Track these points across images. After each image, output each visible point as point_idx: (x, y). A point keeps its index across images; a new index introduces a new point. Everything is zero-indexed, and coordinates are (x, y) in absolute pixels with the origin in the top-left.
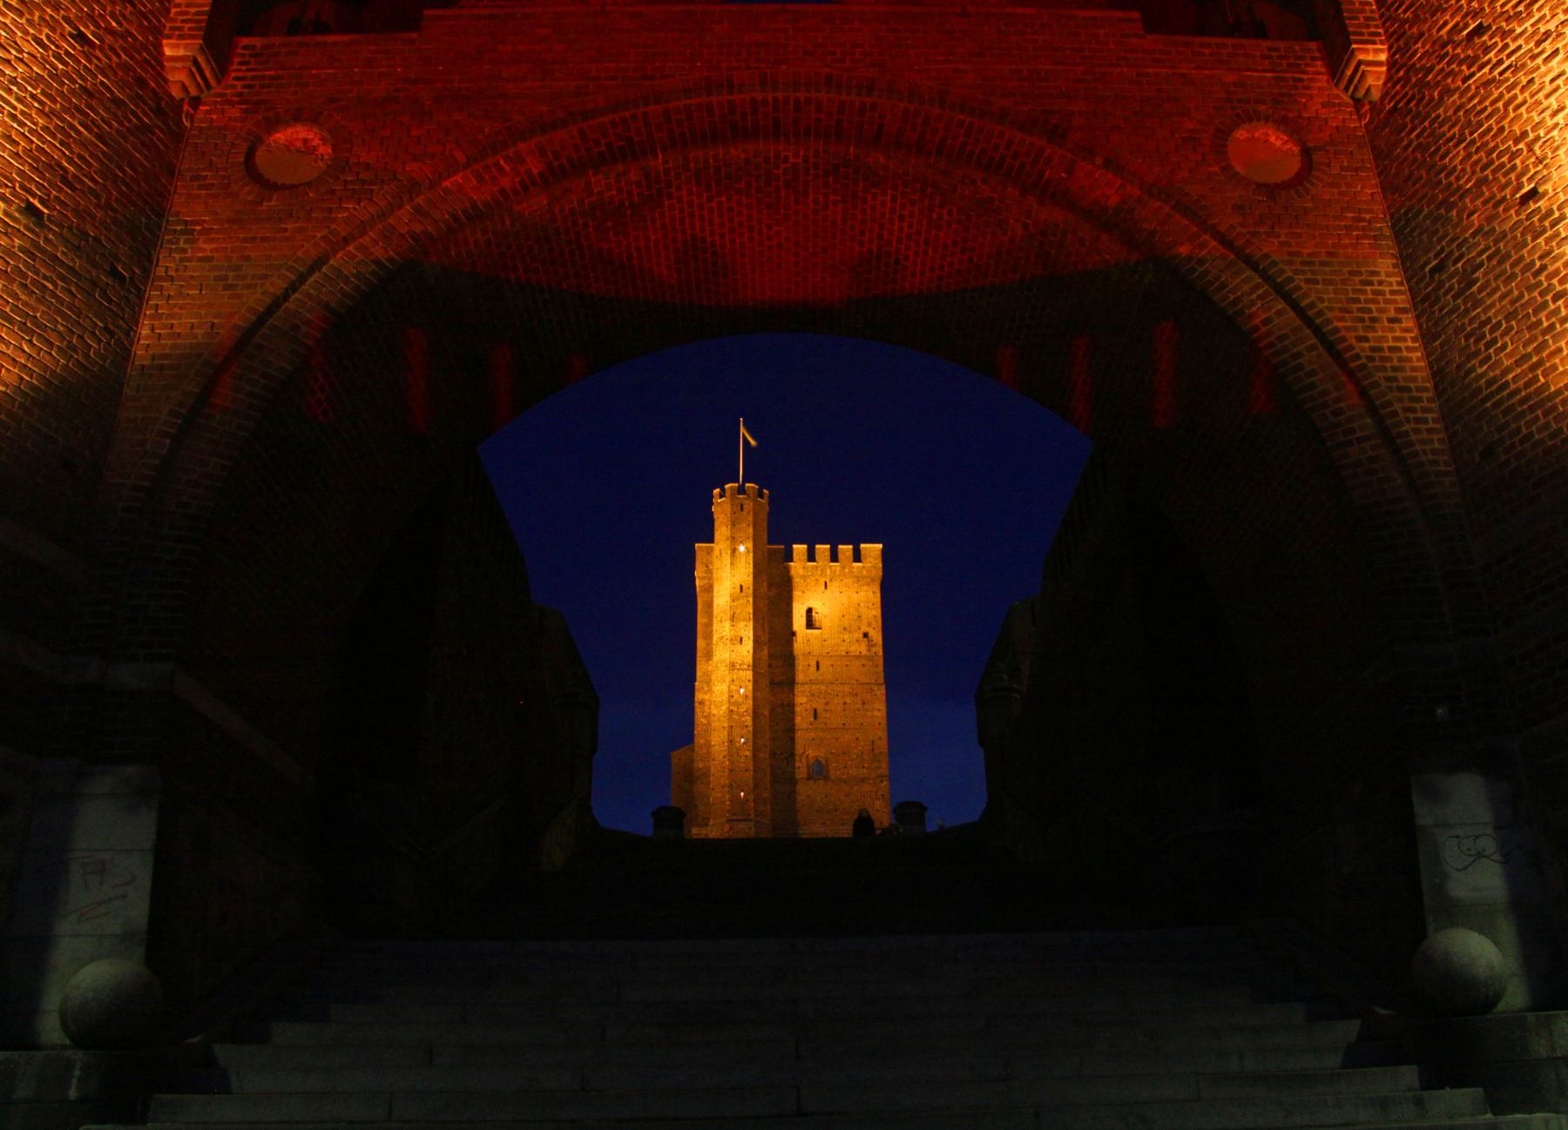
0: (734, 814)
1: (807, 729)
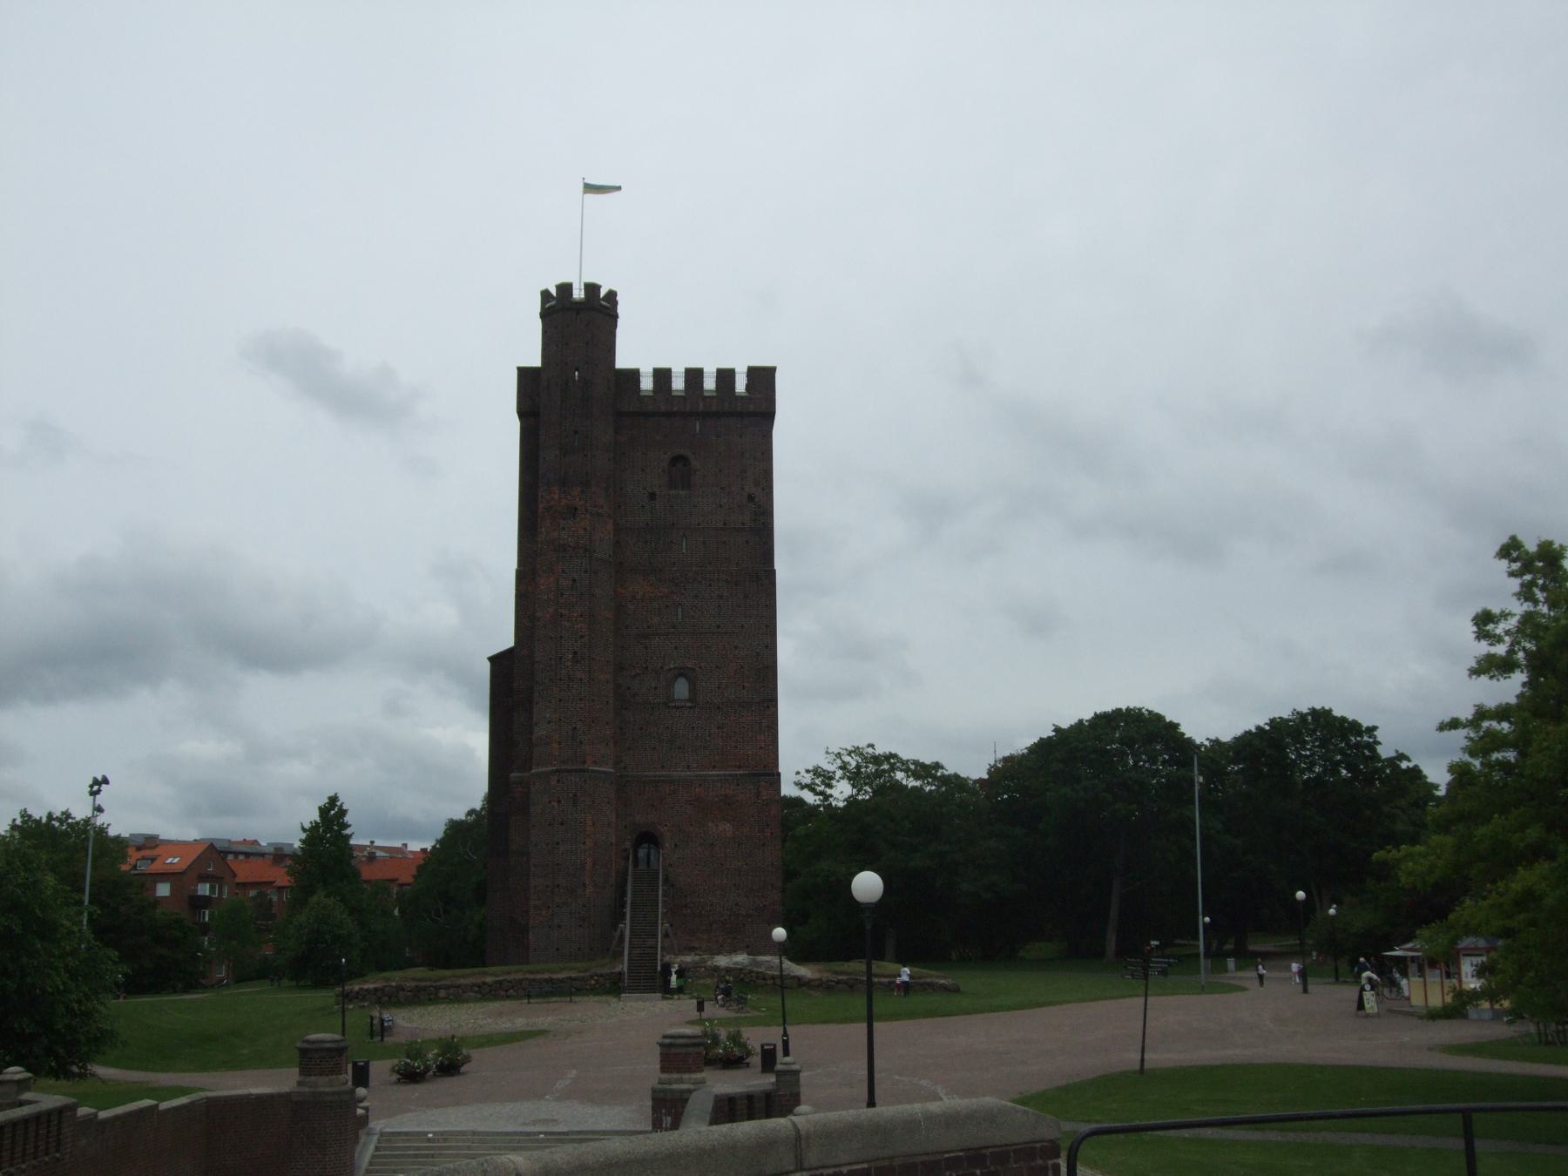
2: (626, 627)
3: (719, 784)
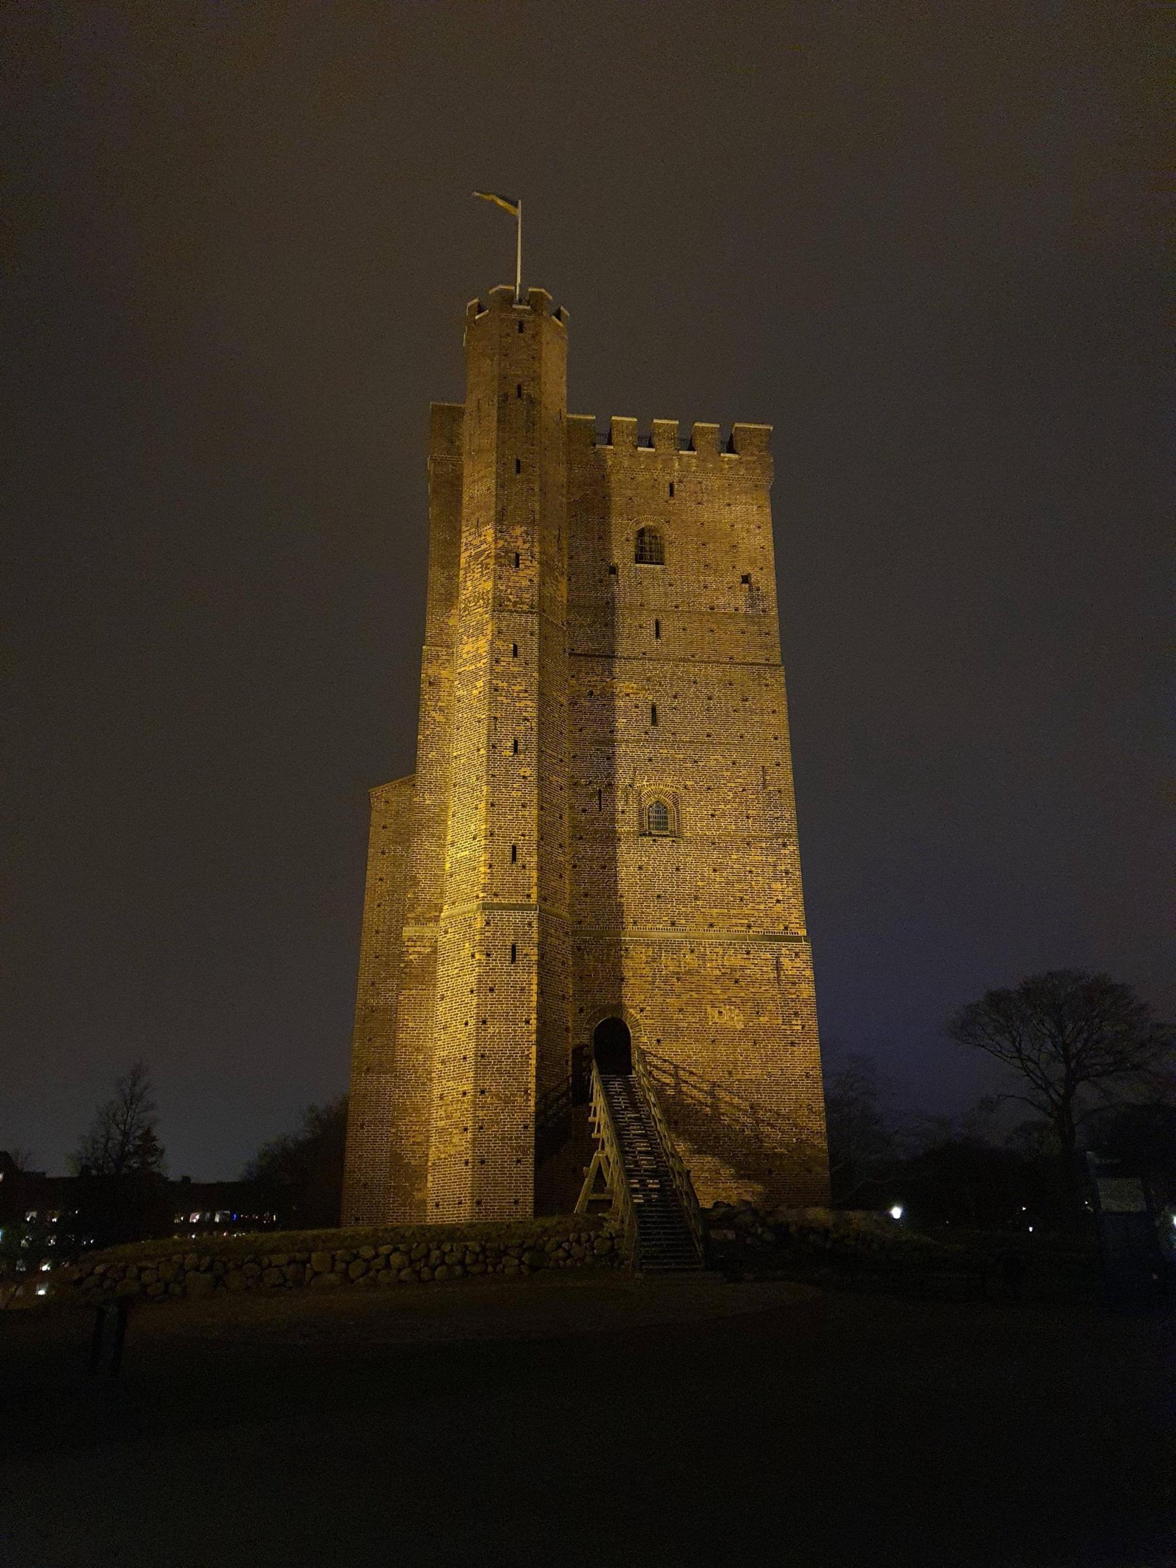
0: (496, 895)
1: (638, 741)
2: (581, 730)
3: (720, 950)
